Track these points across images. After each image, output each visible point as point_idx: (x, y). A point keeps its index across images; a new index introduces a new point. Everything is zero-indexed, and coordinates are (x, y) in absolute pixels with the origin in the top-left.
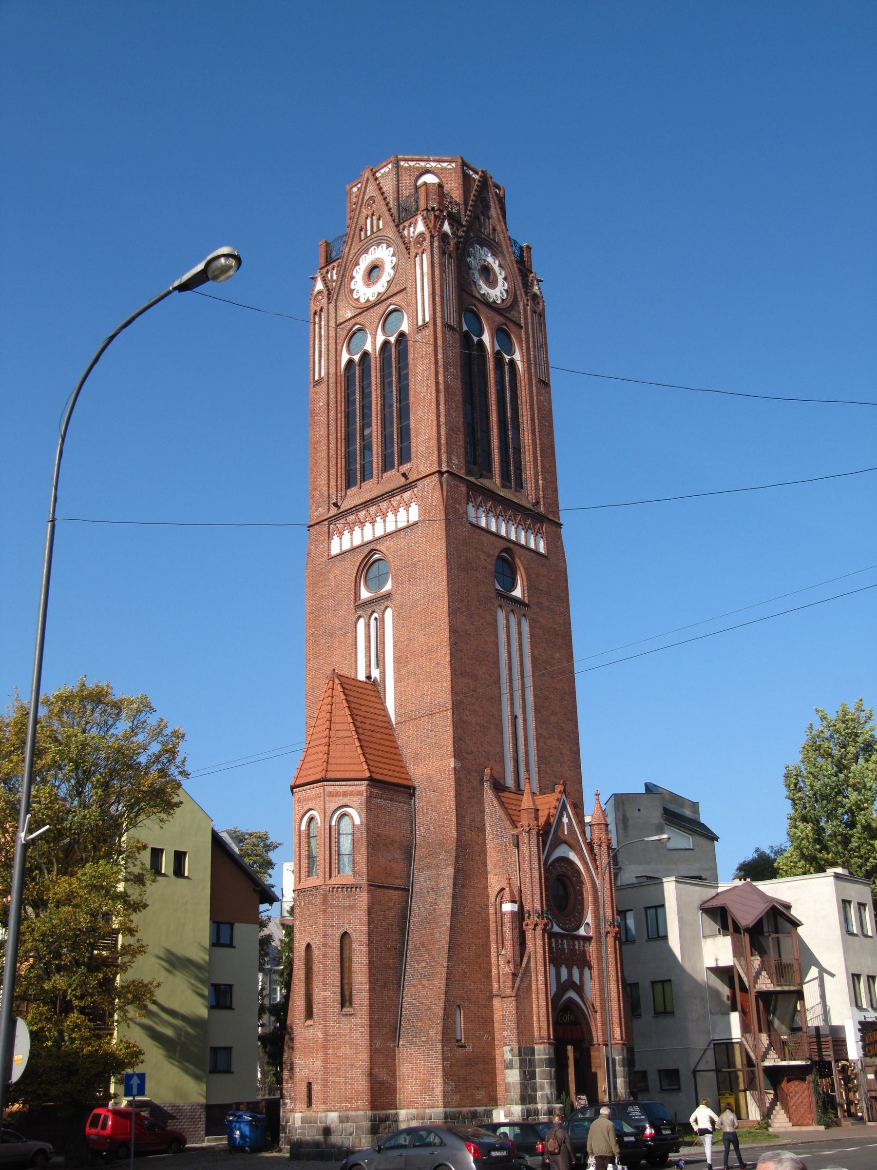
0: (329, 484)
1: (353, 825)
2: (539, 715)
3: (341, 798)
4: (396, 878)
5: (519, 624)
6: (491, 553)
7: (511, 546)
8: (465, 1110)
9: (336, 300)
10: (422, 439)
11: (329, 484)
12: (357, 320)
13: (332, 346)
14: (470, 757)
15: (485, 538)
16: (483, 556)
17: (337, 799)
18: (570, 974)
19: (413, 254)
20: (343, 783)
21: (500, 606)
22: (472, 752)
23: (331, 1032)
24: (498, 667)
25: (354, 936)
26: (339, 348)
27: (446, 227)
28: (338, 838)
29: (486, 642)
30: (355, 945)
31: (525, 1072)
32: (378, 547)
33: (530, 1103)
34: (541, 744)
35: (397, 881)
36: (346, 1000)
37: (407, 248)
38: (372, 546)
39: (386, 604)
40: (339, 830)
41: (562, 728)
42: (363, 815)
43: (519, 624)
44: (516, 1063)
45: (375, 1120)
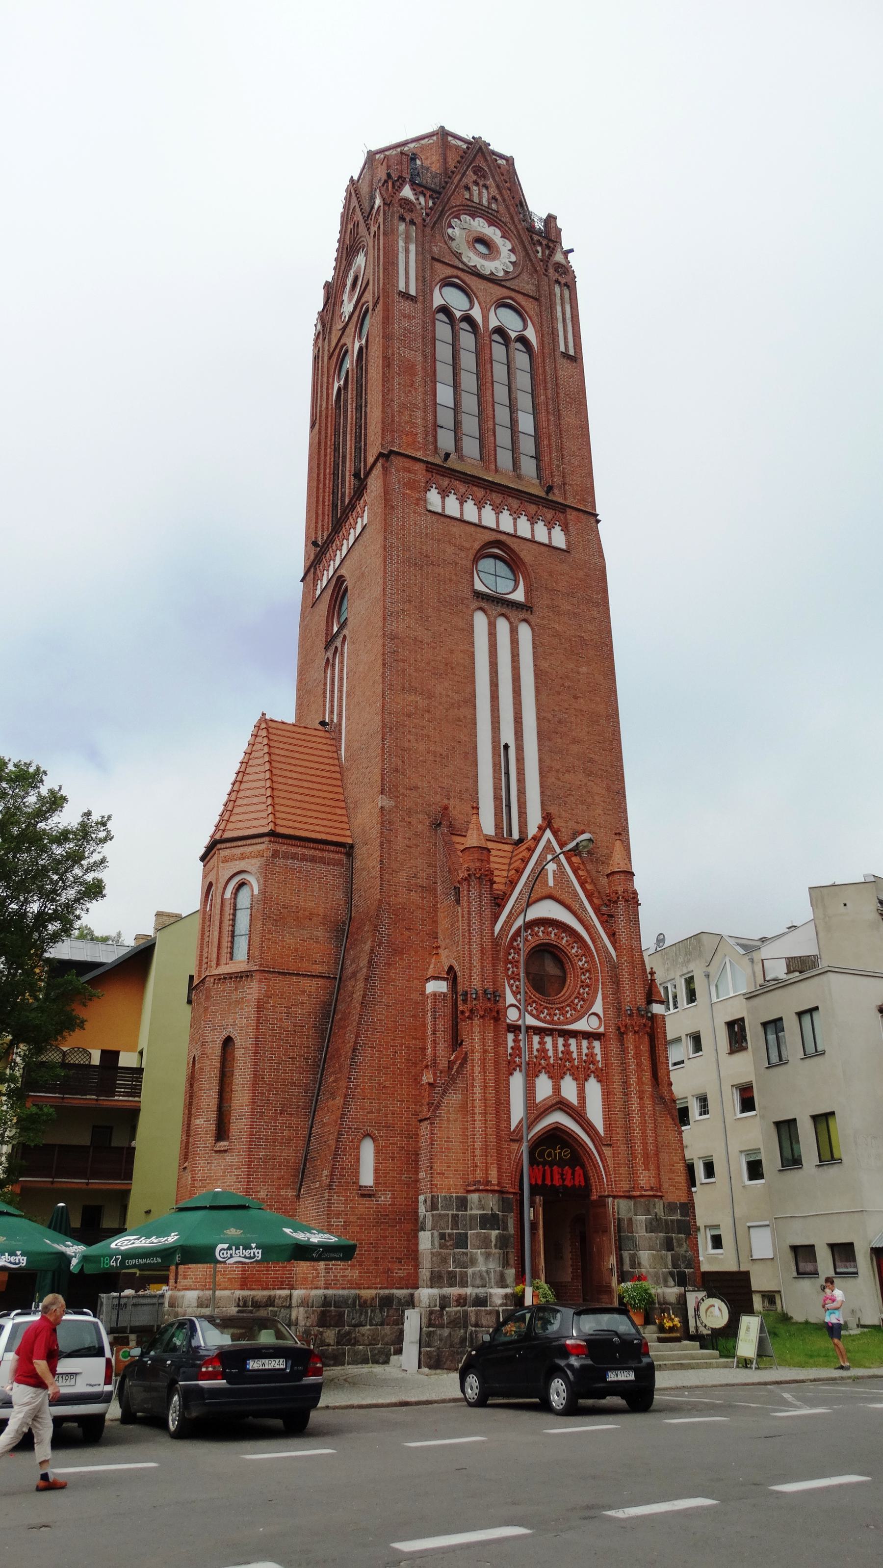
0: (316, 527)
1: (252, 895)
2: (547, 743)
3: (237, 862)
4: (315, 963)
5: (514, 631)
6: (467, 545)
7: (503, 538)
8: (367, 1294)
9: (330, 332)
10: (373, 427)
11: (316, 527)
12: (342, 342)
13: (325, 380)
14: (413, 794)
15: (456, 529)
16: (450, 550)
17: (232, 864)
18: (557, 1089)
19: (372, 235)
20: (240, 843)
21: (481, 609)
22: (416, 788)
23: (199, 1176)
24: (473, 682)
25: (238, 1042)
26: (331, 380)
27: (407, 192)
28: (234, 915)
29: (452, 652)
30: (239, 1053)
31: (442, 1236)
32: (342, 572)
34: (551, 780)
35: (314, 967)
36: (222, 1132)
37: (368, 229)
38: (338, 574)
39: (345, 632)
40: (235, 904)
41: (591, 760)
42: (262, 882)
43: (514, 631)
44: (429, 1224)
45: (245, 1305)
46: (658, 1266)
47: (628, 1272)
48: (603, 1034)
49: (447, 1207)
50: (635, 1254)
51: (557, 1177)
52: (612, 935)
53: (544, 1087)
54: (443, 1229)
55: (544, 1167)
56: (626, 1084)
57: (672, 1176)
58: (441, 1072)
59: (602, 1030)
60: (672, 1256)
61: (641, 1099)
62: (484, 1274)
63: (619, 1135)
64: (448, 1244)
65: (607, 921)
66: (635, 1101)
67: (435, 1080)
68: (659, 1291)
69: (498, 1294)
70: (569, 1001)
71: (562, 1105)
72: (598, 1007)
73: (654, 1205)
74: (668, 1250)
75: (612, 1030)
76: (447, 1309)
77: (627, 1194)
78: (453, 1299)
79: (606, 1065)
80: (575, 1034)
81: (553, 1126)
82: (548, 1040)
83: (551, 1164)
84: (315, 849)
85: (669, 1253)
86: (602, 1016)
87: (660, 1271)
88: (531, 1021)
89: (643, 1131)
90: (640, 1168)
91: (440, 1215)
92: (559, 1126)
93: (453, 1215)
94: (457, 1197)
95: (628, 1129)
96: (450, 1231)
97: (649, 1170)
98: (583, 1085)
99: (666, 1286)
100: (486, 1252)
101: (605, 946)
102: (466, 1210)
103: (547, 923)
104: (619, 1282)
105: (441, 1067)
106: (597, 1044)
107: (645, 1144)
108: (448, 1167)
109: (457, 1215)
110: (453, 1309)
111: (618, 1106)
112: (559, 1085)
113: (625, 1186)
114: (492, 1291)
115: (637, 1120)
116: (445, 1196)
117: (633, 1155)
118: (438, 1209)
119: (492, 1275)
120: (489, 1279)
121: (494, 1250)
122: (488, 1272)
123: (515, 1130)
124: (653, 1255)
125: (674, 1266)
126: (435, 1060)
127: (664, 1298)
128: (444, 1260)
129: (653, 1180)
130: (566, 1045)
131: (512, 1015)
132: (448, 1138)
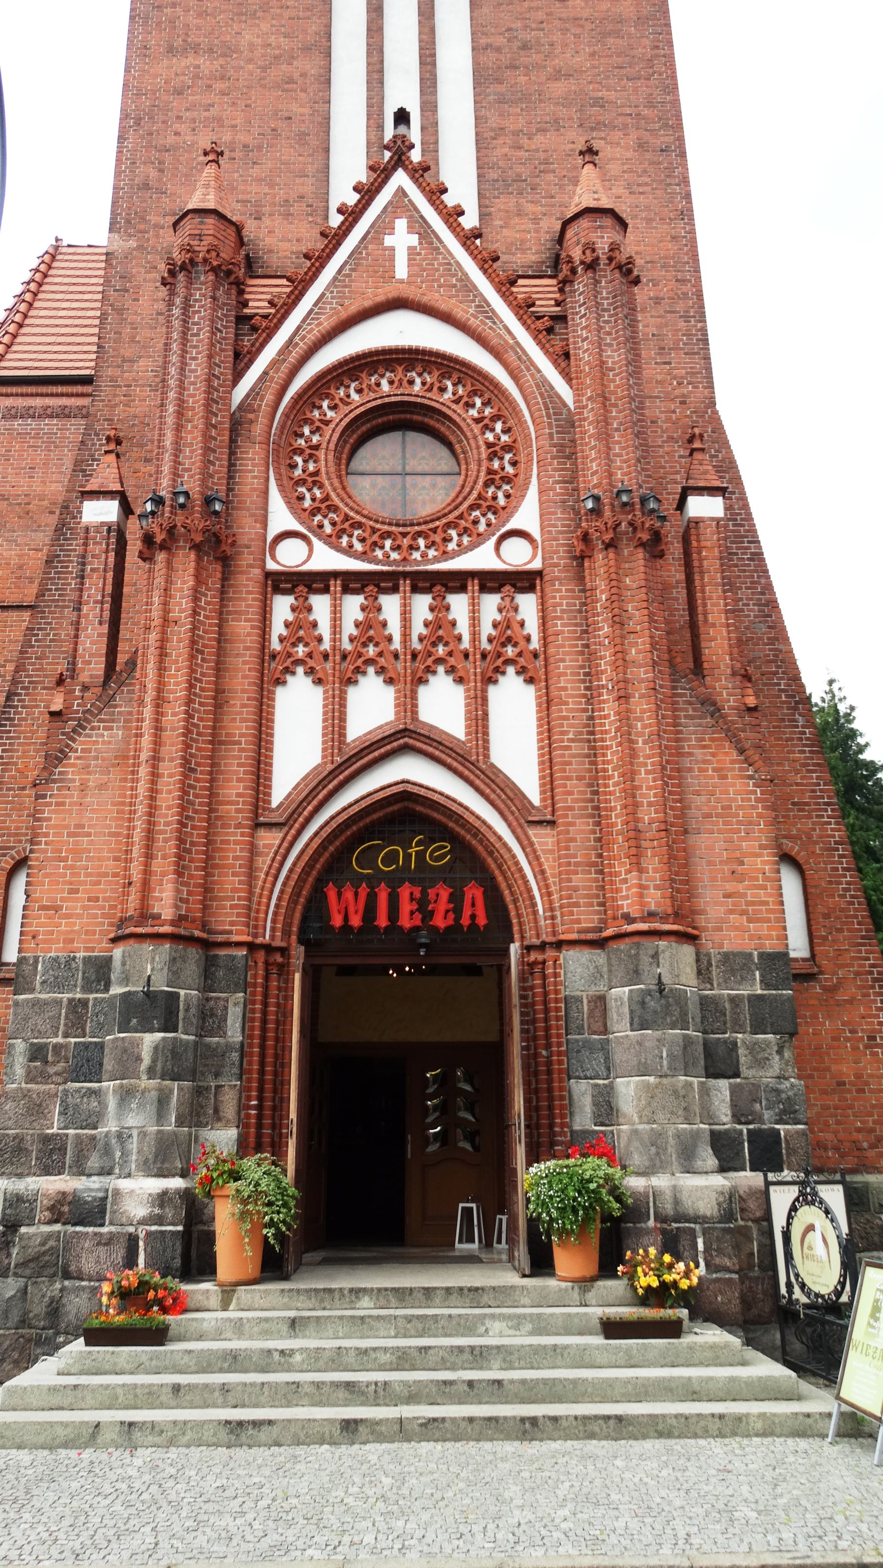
31: (37, 1053)
33: (47, 1171)
46: (660, 1116)
47: (586, 1133)
48: (539, 573)
49: (57, 985)
50: (611, 1087)
51: (406, 907)
52: (563, 359)
53: (371, 706)
54: (40, 1034)
55: (372, 888)
56: (590, 675)
57: (740, 888)
58: (85, 688)
59: (537, 565)
60: (733, 1090)
61: (623, 698)
62: (114, 1141)
63: (573, 792)
64: (51, 1070)
65: (550, 330)
66: (609, 708)
67: (68, 707)
68: (661, 1182)
69: (139, 1193)
70: (456, 513)
71: (407, 737)
72: (527, 515)
73: (655, 956)
74: (713, 1073)
75: (561, 558)
76: (23, 1230)
77: (590, 936)
78: (43, 1202)
79: (545, 638)
80: (458, 581)
81: (395, 790)
82: (390, 606)
83: (394, 881)
84: (67, 395)
85: (723, 1084)
86: (536, 534)
87: (671, 1130)
88: (326, 559)
89: (629, 775)
90: (621, 867)
91: (36, 1003)
92: (410, 788)
93: (71, 1001)
94: (87, 961)
95: (594, 781)
96: (60, 1040)
97: (641, 870)
98: (484, 691)
99: (689, 1170)
100: (121, 1086)
101: (544, 385)
102: (107, 989)
103: (399, 362)
104: (529, 1164)
105: (84, 677)
106: (528, 606)
107: (632, 807)
108: (71, 892)
109: (84, 1003)
110: (36, 1231)
111: (569, 729)
112: (414, 697)
113: (586, 918)
114: (124, 1184)
115: (612, 754)
116: (56, 959)
117: (602, 842)
118: (32, 990)
119: (134, 1145)
120: (125, 1154)
121: (144, 1082)
122: (122, 1137)
123: (279, 807)
124: (648, 1085)
125: (737, 1118)
126: (74, 663)
127: (677, 1202)
128: (37, 1109)
129: (655, 899)
130: (440, 608)
131: (290, 556)
132: (83, 827)
